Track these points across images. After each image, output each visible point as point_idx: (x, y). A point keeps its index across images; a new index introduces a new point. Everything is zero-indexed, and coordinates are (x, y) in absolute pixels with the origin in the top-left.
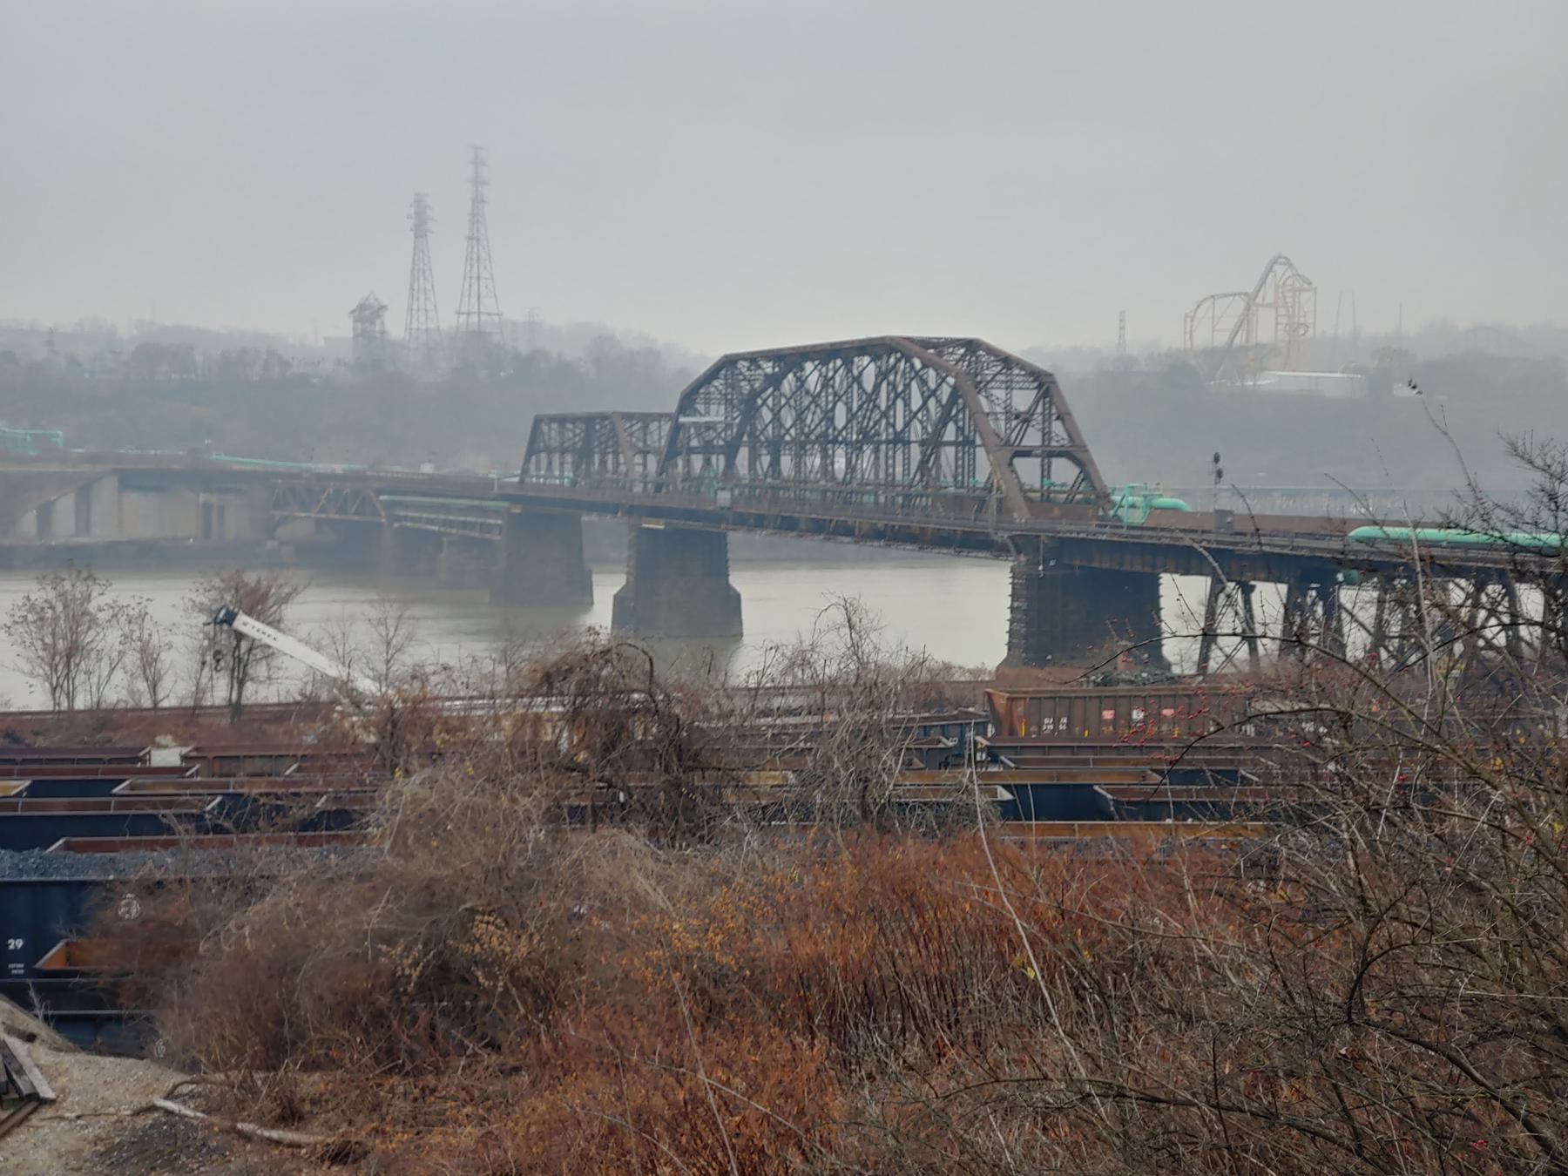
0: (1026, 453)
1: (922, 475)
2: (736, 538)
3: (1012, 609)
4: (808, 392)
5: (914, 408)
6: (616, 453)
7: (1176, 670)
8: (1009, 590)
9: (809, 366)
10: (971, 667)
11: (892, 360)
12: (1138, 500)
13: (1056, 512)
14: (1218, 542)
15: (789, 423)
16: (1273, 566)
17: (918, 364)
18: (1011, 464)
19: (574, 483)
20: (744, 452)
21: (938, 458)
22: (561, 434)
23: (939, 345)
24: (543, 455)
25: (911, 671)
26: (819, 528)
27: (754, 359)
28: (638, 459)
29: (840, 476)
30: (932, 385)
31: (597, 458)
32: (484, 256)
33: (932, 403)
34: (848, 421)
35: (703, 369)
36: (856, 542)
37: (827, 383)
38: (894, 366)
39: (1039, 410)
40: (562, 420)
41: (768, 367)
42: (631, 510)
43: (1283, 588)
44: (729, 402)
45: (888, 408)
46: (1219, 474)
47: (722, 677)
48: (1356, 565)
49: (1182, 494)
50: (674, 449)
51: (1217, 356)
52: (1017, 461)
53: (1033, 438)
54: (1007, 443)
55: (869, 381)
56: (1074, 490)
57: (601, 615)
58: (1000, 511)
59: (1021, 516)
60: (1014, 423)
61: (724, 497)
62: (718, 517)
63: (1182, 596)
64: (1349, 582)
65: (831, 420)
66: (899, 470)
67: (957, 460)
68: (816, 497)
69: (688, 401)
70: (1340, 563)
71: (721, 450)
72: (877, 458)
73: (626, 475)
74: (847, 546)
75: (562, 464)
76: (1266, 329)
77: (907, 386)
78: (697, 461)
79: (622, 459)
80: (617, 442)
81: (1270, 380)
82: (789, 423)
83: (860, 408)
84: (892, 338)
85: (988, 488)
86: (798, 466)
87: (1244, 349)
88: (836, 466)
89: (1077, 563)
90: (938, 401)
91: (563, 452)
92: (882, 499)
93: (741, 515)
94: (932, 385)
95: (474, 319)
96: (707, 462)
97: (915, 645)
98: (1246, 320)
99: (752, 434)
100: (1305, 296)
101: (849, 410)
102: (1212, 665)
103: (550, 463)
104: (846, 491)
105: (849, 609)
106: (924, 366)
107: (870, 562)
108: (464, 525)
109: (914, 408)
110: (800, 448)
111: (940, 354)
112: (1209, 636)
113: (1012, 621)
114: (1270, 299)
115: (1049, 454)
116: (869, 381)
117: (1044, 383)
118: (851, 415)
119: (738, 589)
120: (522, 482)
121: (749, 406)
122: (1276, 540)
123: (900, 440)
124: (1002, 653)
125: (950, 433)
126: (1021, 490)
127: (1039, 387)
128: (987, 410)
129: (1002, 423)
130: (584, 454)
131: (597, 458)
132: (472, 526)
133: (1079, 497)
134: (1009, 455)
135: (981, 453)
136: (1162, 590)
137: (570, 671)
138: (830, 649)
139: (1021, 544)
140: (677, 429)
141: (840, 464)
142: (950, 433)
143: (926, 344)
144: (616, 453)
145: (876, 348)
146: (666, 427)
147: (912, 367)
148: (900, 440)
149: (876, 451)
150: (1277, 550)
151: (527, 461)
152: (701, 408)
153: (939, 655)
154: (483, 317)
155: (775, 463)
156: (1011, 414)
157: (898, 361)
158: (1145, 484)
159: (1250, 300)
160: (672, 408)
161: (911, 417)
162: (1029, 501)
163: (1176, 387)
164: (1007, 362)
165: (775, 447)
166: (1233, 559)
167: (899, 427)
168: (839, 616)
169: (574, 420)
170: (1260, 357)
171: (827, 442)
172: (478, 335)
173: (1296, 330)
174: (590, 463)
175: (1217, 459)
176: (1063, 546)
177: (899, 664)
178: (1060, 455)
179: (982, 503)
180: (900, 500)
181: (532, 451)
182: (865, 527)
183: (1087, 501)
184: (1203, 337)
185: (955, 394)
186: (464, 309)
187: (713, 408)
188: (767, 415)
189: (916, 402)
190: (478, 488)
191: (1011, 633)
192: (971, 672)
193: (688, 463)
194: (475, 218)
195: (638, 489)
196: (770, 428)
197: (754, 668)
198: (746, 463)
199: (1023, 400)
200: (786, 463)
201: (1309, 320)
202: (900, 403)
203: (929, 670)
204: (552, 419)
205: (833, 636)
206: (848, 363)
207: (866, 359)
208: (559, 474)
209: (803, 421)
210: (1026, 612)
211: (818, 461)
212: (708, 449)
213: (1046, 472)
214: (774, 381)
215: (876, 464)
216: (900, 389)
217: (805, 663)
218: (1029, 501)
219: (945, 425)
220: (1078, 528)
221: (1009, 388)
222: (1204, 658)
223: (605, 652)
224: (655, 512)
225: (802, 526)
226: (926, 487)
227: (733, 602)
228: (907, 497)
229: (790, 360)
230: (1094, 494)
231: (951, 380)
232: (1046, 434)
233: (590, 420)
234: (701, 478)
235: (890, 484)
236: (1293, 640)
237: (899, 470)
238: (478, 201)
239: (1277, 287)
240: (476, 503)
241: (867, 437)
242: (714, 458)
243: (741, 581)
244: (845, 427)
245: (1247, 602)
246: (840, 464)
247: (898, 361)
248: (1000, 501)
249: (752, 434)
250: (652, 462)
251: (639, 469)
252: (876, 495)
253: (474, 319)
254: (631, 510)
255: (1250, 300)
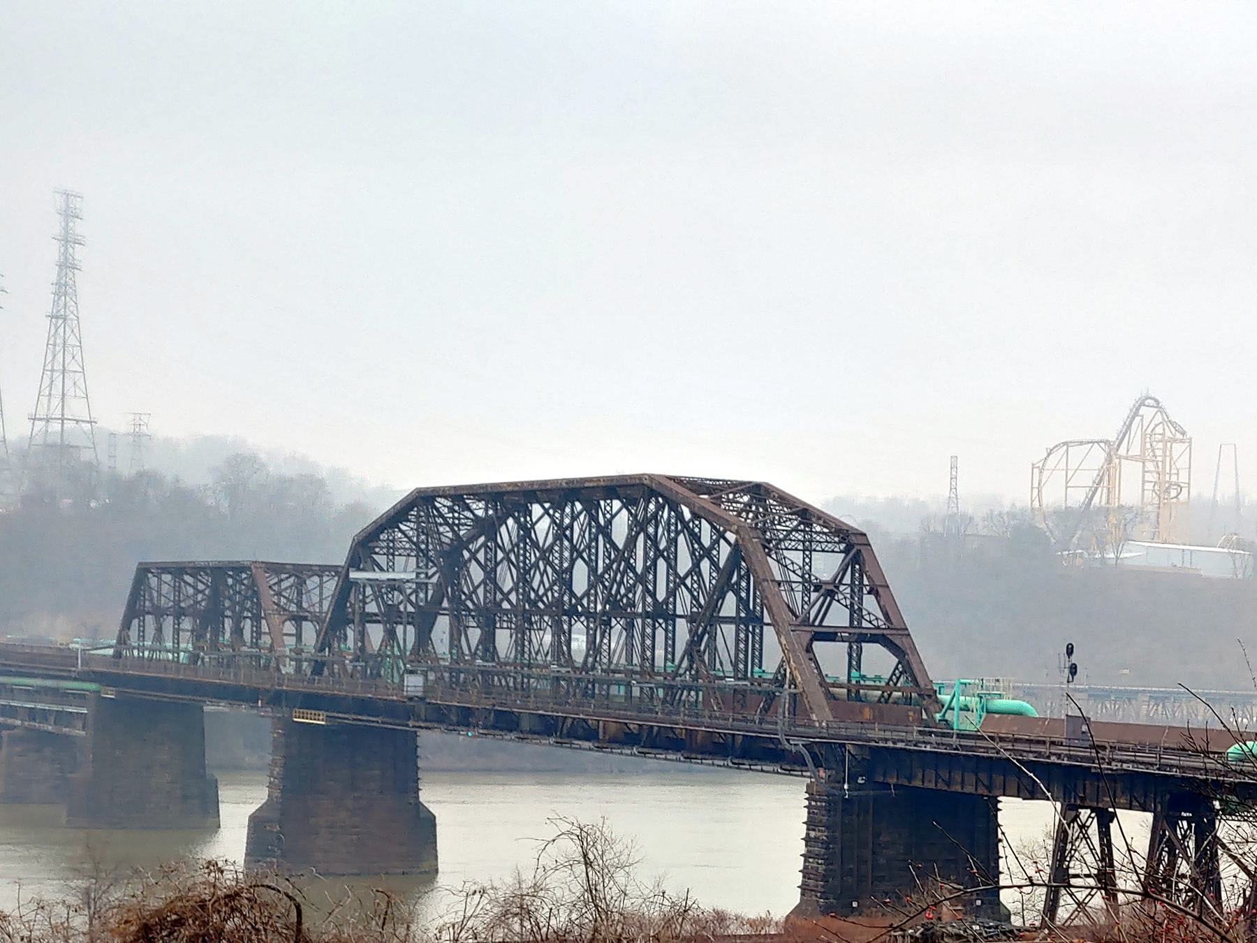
0: (830, 636)
1: (691, 661)
2: (430, 739)
3: (807, 840)
4: (535, 544)
5: (682, 571)
6: (257, 619)
7: (1016, 921)
8: (804, 815)
9: (537, 510)
10: (752, 916)
11: (652, 507)
12: (973, 702)
13: (867, 713)
14: (1070, 757)
15: (508, 585)
16: (1140, 789)
17: (687, 515)
18: (809, 649)
19: (194, 658)
20: (443, 624)
21: (713, 638)
22: (177, 590)
23: (715, 489)
24: (149, 619)
25: (668, 922)
26: (548, 728)
27: (459, 496)
28: (289, 627)
29: (579, 659)
30: (706, 542)
31: (228, 624)
32: (72, 341)
33: (705, 565)
34: (592, 586)
35: (385, 506)
36: (600, 748)
37: (562, 532)
38: (655, 516)
39: (847, 580)
40: (178, 571)
41: (479, 508)
42: (277, 699)
43: (1149, 816)
44: (422, 554)
45: (646, 569)
46: (1073, 670)
47: (401, 931)
48: (1235, 788)
49: (1028, 694)
50: (343, 614)
51: (1084, 515)
52: (818, 646)
53: (838, 617)
54: (806, 622)
55: (621, 529)
56: (891, 684)
57: (230, 845)
58: (793, 711)
59: (821, 717)
60: (814, 596)
61: (414, 683)
62: (405, 710)
63: (1026, 824)
64: (1229, 811)
65: (569, 584)
66: (660, 653)
67: (737, 640)
68: (545, 686)
69: (365, 548)
70: (1218, 785)
71: (410, 619)
72: (630, 637)
73: (271, 649)
74: (586, 753)
75: (177, 632)
76: (1132, 487)
77: (673, 542)
78: (376, 633)
79: (265, 628)
80: (259, 605)
81: (1134, 554)
82: (508, 585)
83: (608, 568)
84: (651, 477)
85: (779, 681)
86: (520, 645)
87: (1106, 512)
88: (574, 645)
89: (893, 781)
90: (714, 564)
91: (179, 614)
92: (636, 692)
93: (438, 708)
94: (706, 542)
95: (56, 426)
96: (391, 634)
97: (674, 891)
98: (1107, 476)
99: (457, 601)
100: (1178, 448)
101: (593, 570)
102: (1062, 914)
103: (159, 630)
104: (587, 679)
105: (582, 836)
106: (696, 516)
107: (619, 775)
108: (32, 714)
109: (682, 571)
110: (524, 621)
111: (717, 502)
112: (1060, 878)
113: (806, 857)
114: (1136, 450)
115: (858, 638)
116: (621, 529)
117: (854, 545)
118: (595, 579)
119: (433, 808)
120: (118, 655)
121: (452, 561)
122: (1119, 755)
123: (663, 614)
124: (793, 898)
125: (729, 606)
126: (823, 683)
127: (846, 551)
128: (778, 578)
129: (799, 596)
130: (209, 619)
131: (228, 624)
132: (45, 715)
133: (896, 694)
134: (809, 636)
135: (769, 632)
136: (1002, 818)
137: (180, 922)
138: (559, 893)
139: (818, 756)
140: (347, 587)
141: (579, 643)
142: (729, 606)
143: (697, 486)
144: (257, 619)
145: (632, 490)
146: (331, 585)
147: (680, 516)
148: (663, 614)
149: (629, 627)
150: (1142, 769)
151: (126, 625)
152: (382, 560)
153: (706, 901)
154: (69, 425)
155: (488, 639)
156: (810, 584)
157: (660, 507)
158: (982, 680)
159: (1112, 450)
160: (341, 559)
161: (677, 582)
162: (832, 697)
163: (1028, 557)
164: (805, 514)
165: (489, 618)
166: (1084, 780)
167: (661, 596)
168: (571, 848)
169: (196, 570)
170: (1124, 522)
171: (564, 612)
172: (62, 449)
173: (1167, 490)
174: (219, 631)
175: (1070, 651)
176: (878, 759)
177: (655, 913)
178: (874, 639)
179: (771, 698)
180: (661, 693)
181: (134, 611)
182: (613, 728)
183: (908, 701)
184: (1053, 496)
185: (737, 553)
186: (42, 413)
187: (400, 561)
188: (477, 574)
189: (684, 564)
190: (58, 663)
191: (806, 872)
192: (752, 923)
193: (362, 635)
194: (63, 289)
195: (288, 669)
196: (480, 591)
197: (449, 919)
198: (446, 637)
199: (826, 565)
200: (504, 640)
201: (1183, 478)
202: (662, 564)
203: (696, 921)
204: (164, 569)
205: (563, 874)
206: (592, 508)
207: (617, 504)
208: (172, 645)
209: (527, 583)
210: (826, 845)
211: (548, 638)
212: (391, 617)
213: (854, 661)
214: (488, 528)
215: (629, 646)
216: (663, 545)
217: (525, 913)
218: (832, 697)
219: (722, 597)
220: (895, 736)
221: (808, 550)
222: (1051, 907)
223: (233, 896)
224: (312, 702)
225: (525, 725)
226: (695, 678)
227: (430, 822)
228: (669, 688)
229: (511, 500)
230: (915, 691)
231: (731, 537)
232: (856, 612)
233: (218, 571)
234: (381, 655)
235: (648, 670)
236: (1155, 883)
237: (660, 653)
238: (67, 265)
239: (1144, 436)
240: (49, 683)
241: (618, 608)
242: (399, 629)
243: (431, 796)
244: (587, 594)
245: (1105, 833)
246: (579, 643)
247: (660, 507)
248: (794, 696)
249: (457, 601)
250: (310, 633)
251: (291, 641)
252: (629, 685)
253: (56, 426)
254: (277, 699)
255: (1112, 450)
